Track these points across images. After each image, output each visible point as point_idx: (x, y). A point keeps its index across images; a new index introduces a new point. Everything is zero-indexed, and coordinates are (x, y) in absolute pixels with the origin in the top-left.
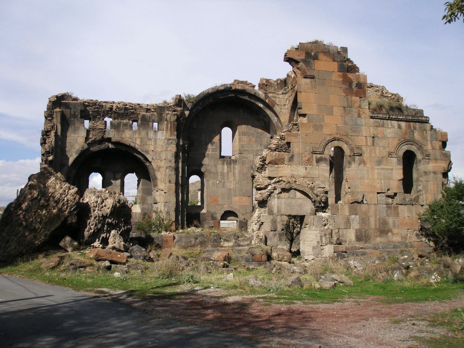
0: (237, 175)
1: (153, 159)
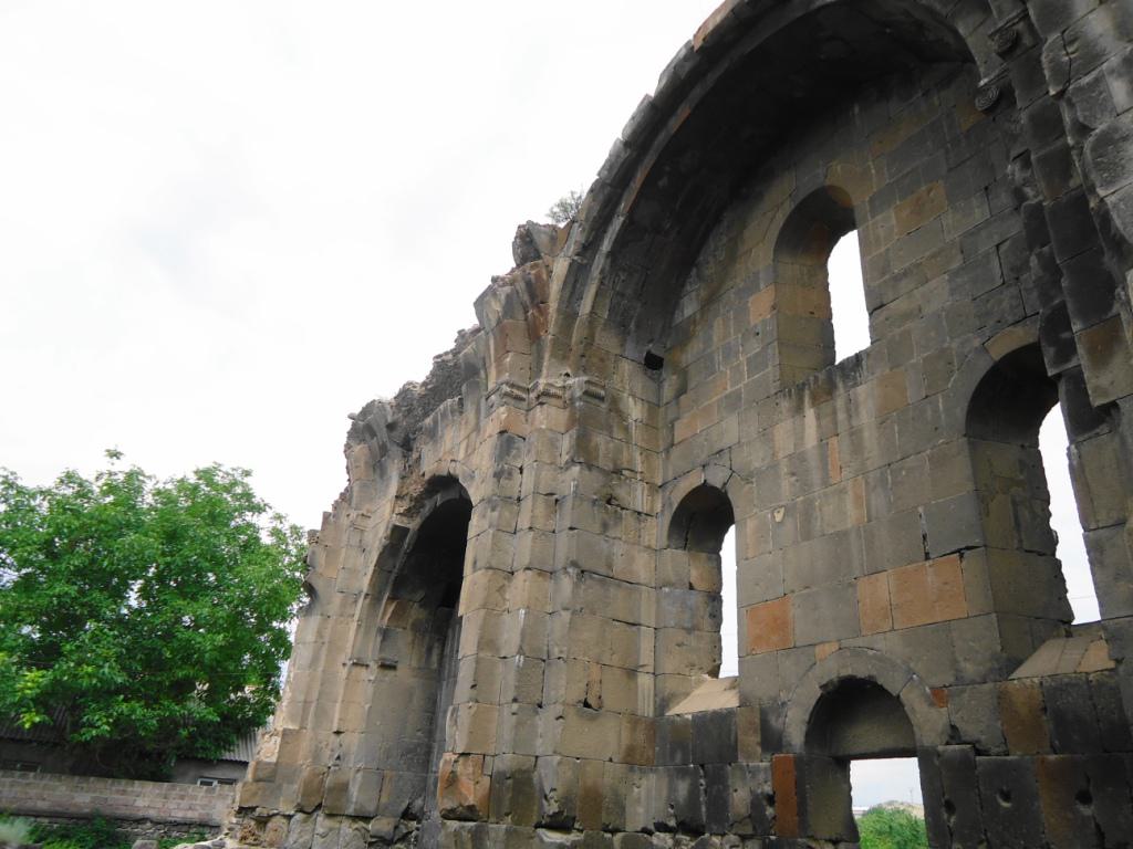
0: (870, 437)
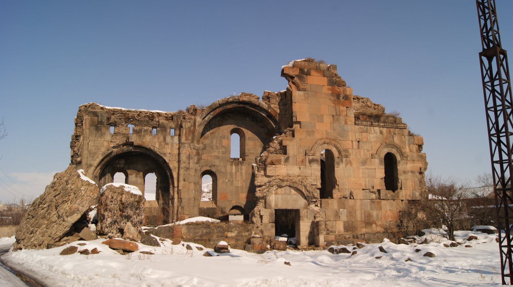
0: (244, 174)
1: (170, 160)
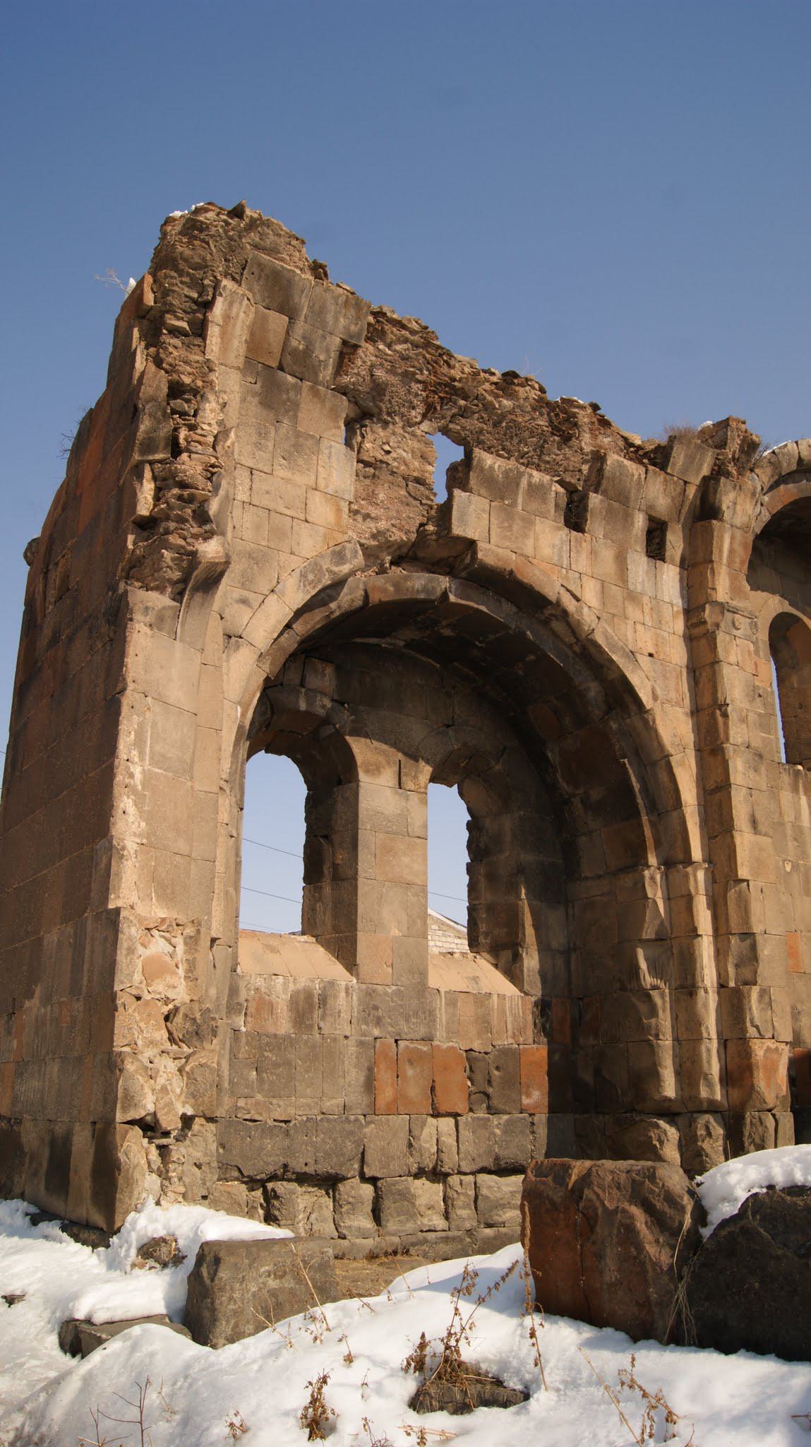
1: (655, 698)
